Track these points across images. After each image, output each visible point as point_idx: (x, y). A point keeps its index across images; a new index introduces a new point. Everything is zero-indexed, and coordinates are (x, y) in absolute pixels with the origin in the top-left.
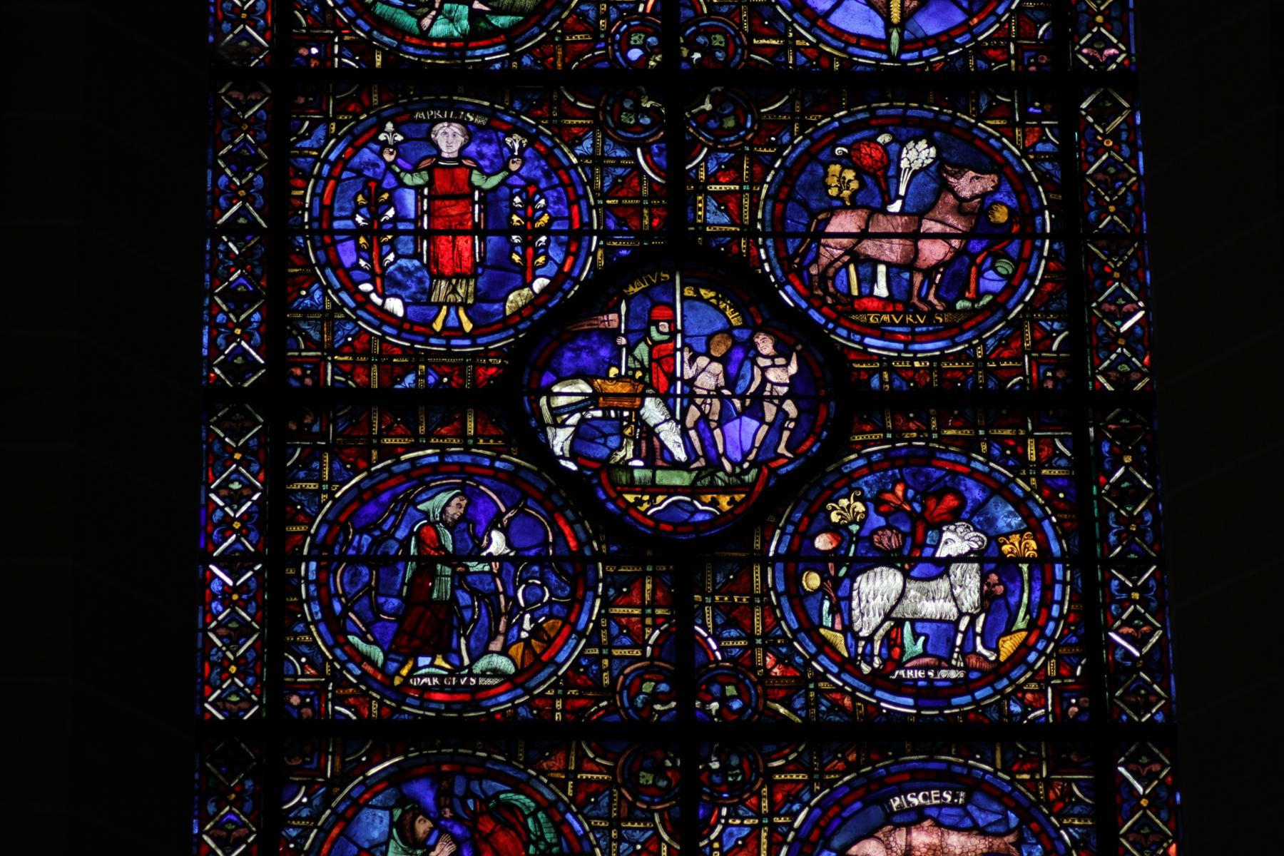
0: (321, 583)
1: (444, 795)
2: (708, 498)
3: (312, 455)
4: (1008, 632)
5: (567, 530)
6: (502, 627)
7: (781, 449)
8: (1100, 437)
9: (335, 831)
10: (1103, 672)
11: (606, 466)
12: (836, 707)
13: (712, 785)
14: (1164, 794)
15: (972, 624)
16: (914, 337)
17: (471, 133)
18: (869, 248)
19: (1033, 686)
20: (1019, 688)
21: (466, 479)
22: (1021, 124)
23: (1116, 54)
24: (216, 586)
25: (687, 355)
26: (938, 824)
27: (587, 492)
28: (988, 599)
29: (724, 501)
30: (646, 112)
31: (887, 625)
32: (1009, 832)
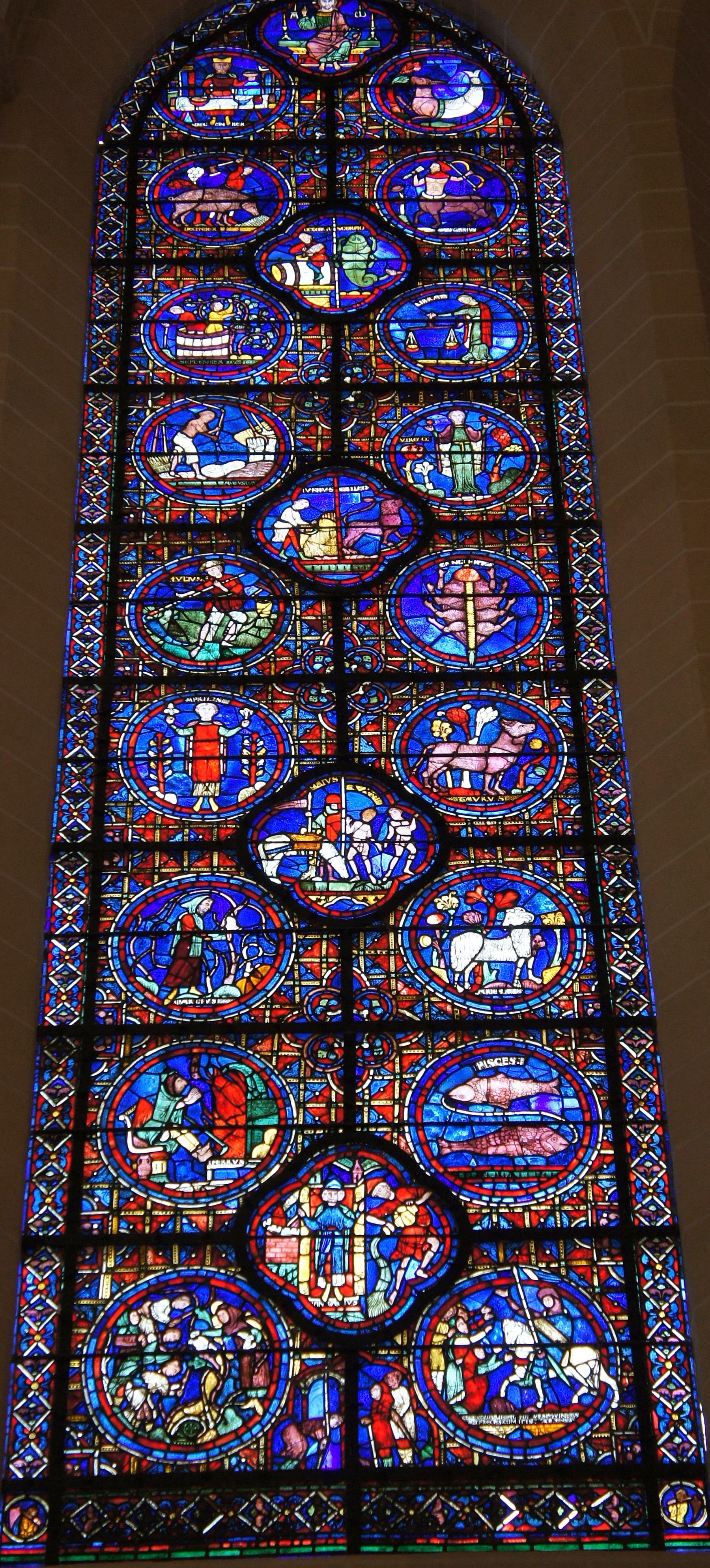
0: (121, 949)
2: (361, 897)
3: (120, 878)
4: (548, 967)
5: (274, 916)
6: (233, 971)
7: (407, 870)
8: (602, 860)
9: (124, 1088)
10: (607, 991)
11: (298, 881)
13: (364, 1057)
14: (649, 1057)
15: (526, 963)
16: (486, 808)
18: (458, 762)
19: (565, 997)
20: (556, 999)
22: (548, 698)
23: (603, 662)
24: (55, 952)
25: (349, 820)
26: (507, 1076)
29: (371, 899)
30: (324, 695)
31: (474, 964)
32: (553, 1080)
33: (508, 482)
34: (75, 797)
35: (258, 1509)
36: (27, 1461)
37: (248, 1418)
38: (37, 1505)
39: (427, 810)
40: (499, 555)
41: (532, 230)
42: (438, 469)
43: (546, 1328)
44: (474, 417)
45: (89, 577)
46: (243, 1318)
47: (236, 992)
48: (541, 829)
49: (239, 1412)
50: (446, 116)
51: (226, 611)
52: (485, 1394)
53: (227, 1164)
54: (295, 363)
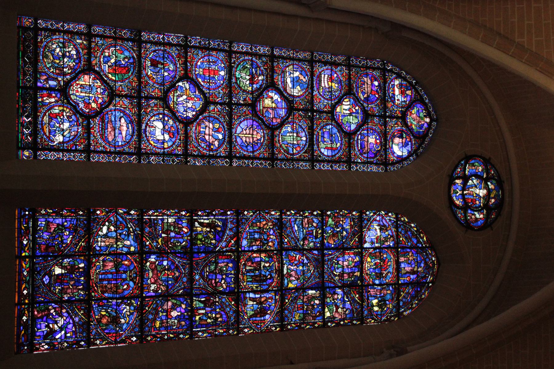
0: (160, 50)
1: (131, 63)
3: (178, 50)
11: (177, 90)
12: (143, 118)
16: (195, 133)
17: (223, 76)
18: (207, 128)
21: (175, 71)
23: (234, 165)
27: (173, 87)
28: (159, 140)
29: (172, 105)
33: (285, 148)
34: (200, 42)
35: (29, 69)
36: (41, 23)
37: (49, 69)
38: (32, 25)
39: (195, 120)
40: (264, 144)
41: (359, 163)
42: (289, 132)
43: (67, 132)
44: (304, 143)
45: (259, 50)
46: (71, 69)
47: (149, 74)
48: (190, 145)
49: (51, 67)
50: (393, 145)
51: (249, 79)
52: (52, 117)
53: (107, 68)
54: (320, 102)
